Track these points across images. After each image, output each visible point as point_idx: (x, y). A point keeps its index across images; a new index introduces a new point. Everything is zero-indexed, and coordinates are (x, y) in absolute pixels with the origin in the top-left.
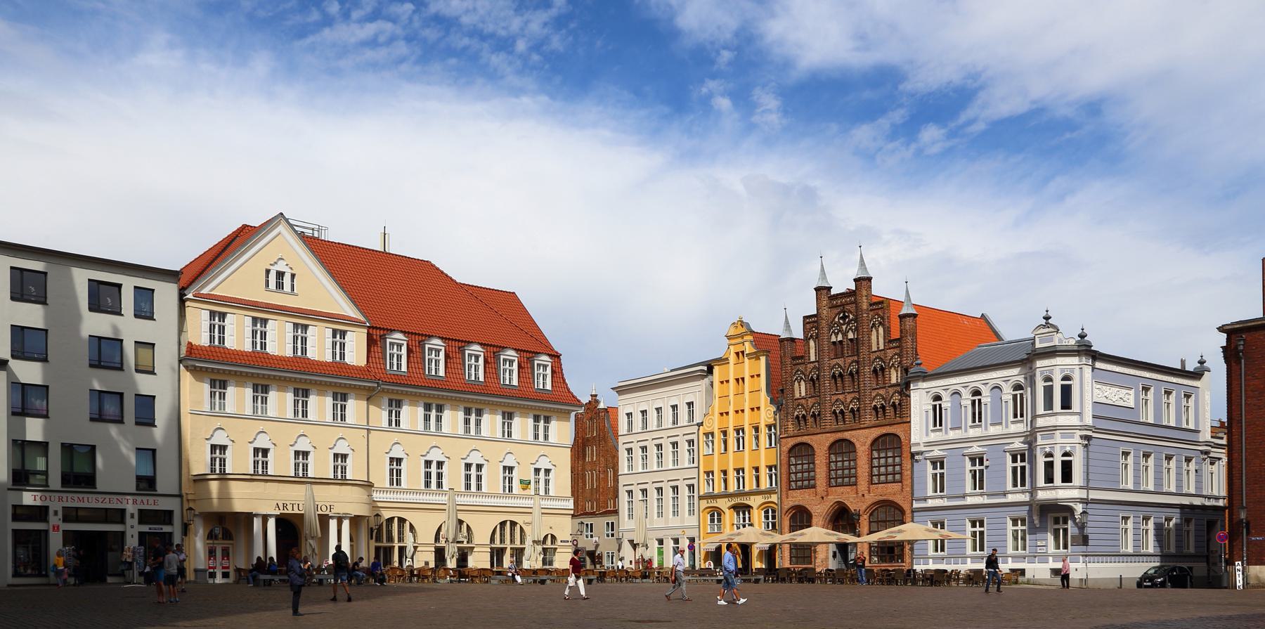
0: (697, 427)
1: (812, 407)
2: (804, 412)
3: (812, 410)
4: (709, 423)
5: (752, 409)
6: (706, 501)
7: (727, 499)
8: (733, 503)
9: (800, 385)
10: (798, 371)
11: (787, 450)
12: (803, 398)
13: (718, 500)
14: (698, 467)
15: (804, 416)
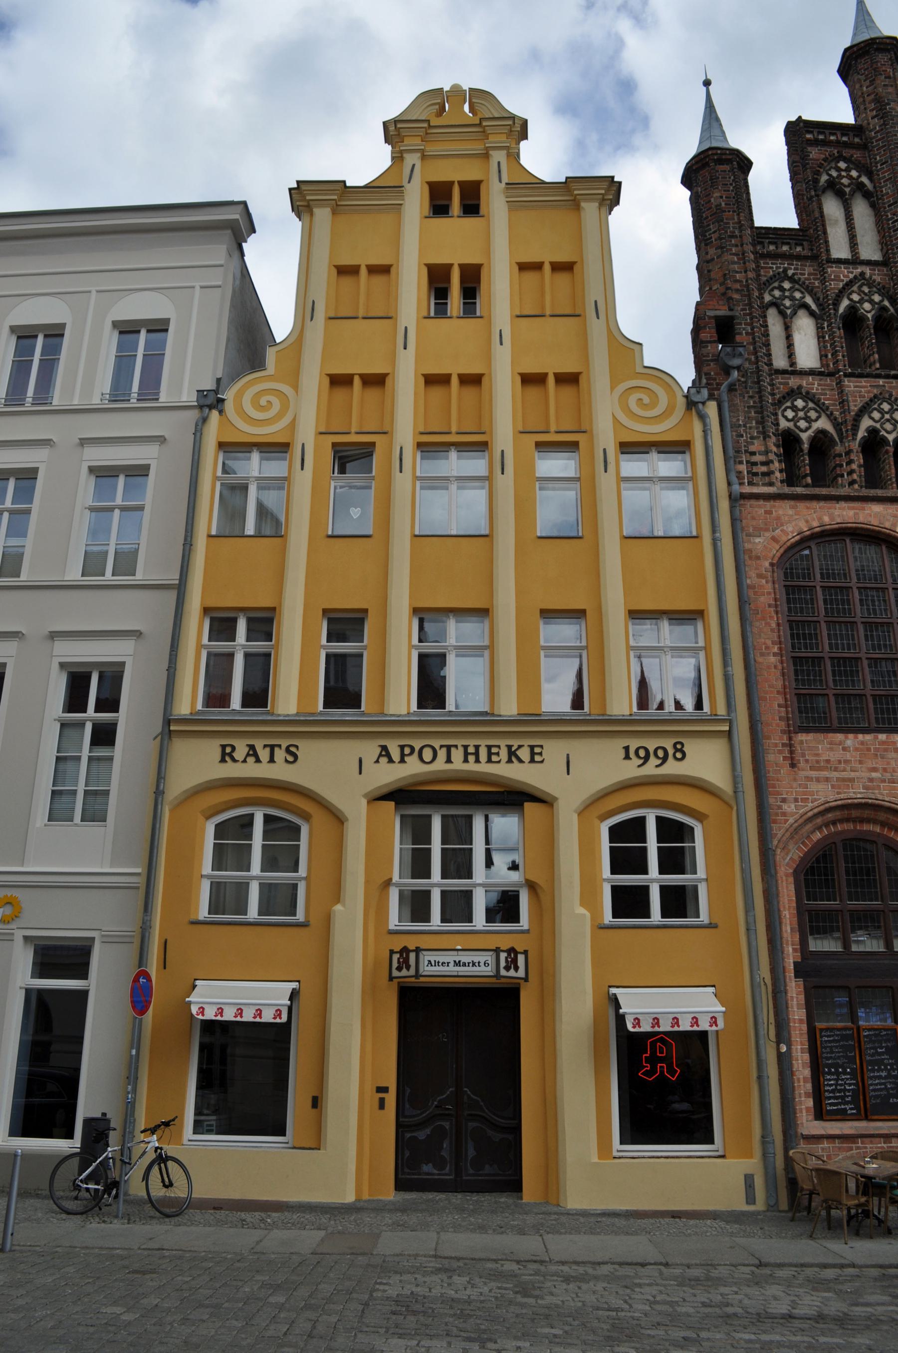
0: (194, 415)
1: (865, 410)
2: (823, 423)
3: (866, 423)
4: (262, 408)
5: (530, 380)
6: (213, 748)
7: (370, 750)
8: (413, 768)
9: (787, 328)
10: (784, 276)
11: (775, 550)
12: (811, 372)
13: (305, 748)
14: (181, 588)
15: (821, 442)
